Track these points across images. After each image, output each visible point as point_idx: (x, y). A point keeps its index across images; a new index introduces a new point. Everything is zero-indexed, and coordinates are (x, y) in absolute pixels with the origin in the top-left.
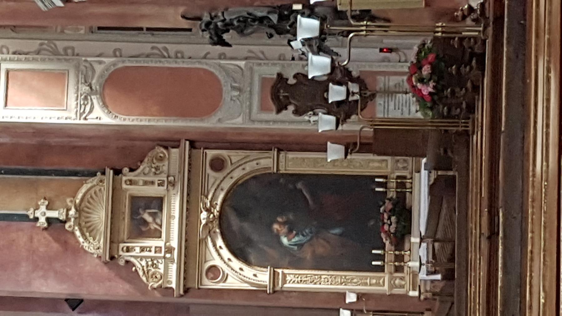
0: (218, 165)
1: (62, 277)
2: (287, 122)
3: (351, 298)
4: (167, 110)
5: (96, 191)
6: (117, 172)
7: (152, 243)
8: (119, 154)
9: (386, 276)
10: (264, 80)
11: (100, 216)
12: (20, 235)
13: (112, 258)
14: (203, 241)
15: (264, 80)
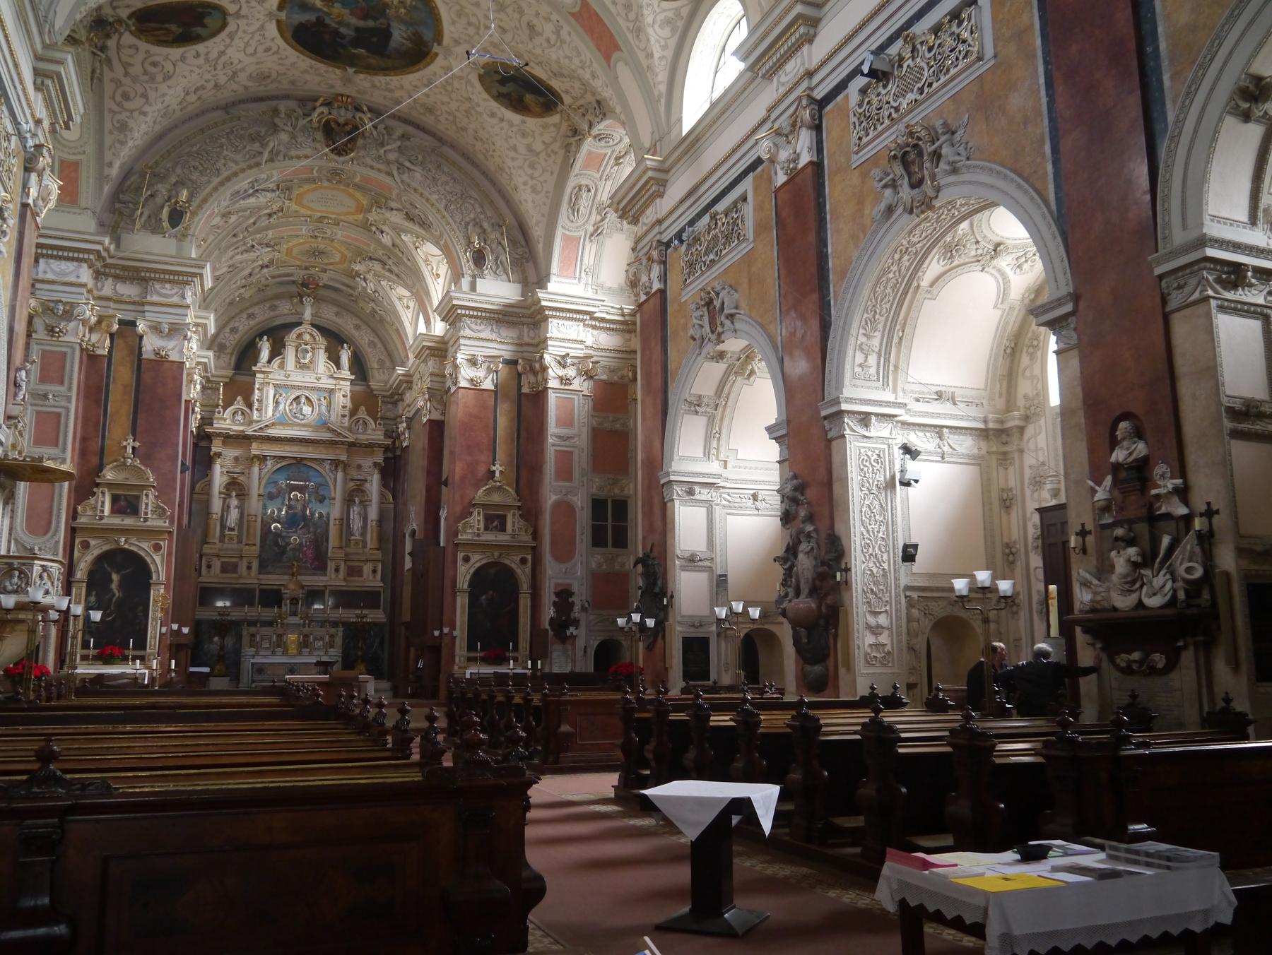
0: (523, 561)
1: (463, 478)
2: (548, 598)
3: (455, 633)
4: (553, 535)
5: (508, 497)
6: (519, 508)
7: (482, 526)
8: (530, 514)
9: (465, 652)
10: (570, 585)
11: (496, 498)
12: (484, 457)
13: (474, 505)
14: (483, 553)
15: (570, 585)
